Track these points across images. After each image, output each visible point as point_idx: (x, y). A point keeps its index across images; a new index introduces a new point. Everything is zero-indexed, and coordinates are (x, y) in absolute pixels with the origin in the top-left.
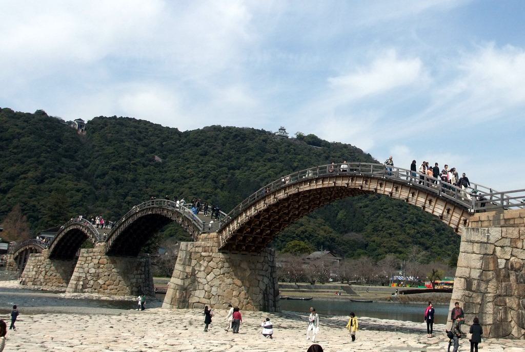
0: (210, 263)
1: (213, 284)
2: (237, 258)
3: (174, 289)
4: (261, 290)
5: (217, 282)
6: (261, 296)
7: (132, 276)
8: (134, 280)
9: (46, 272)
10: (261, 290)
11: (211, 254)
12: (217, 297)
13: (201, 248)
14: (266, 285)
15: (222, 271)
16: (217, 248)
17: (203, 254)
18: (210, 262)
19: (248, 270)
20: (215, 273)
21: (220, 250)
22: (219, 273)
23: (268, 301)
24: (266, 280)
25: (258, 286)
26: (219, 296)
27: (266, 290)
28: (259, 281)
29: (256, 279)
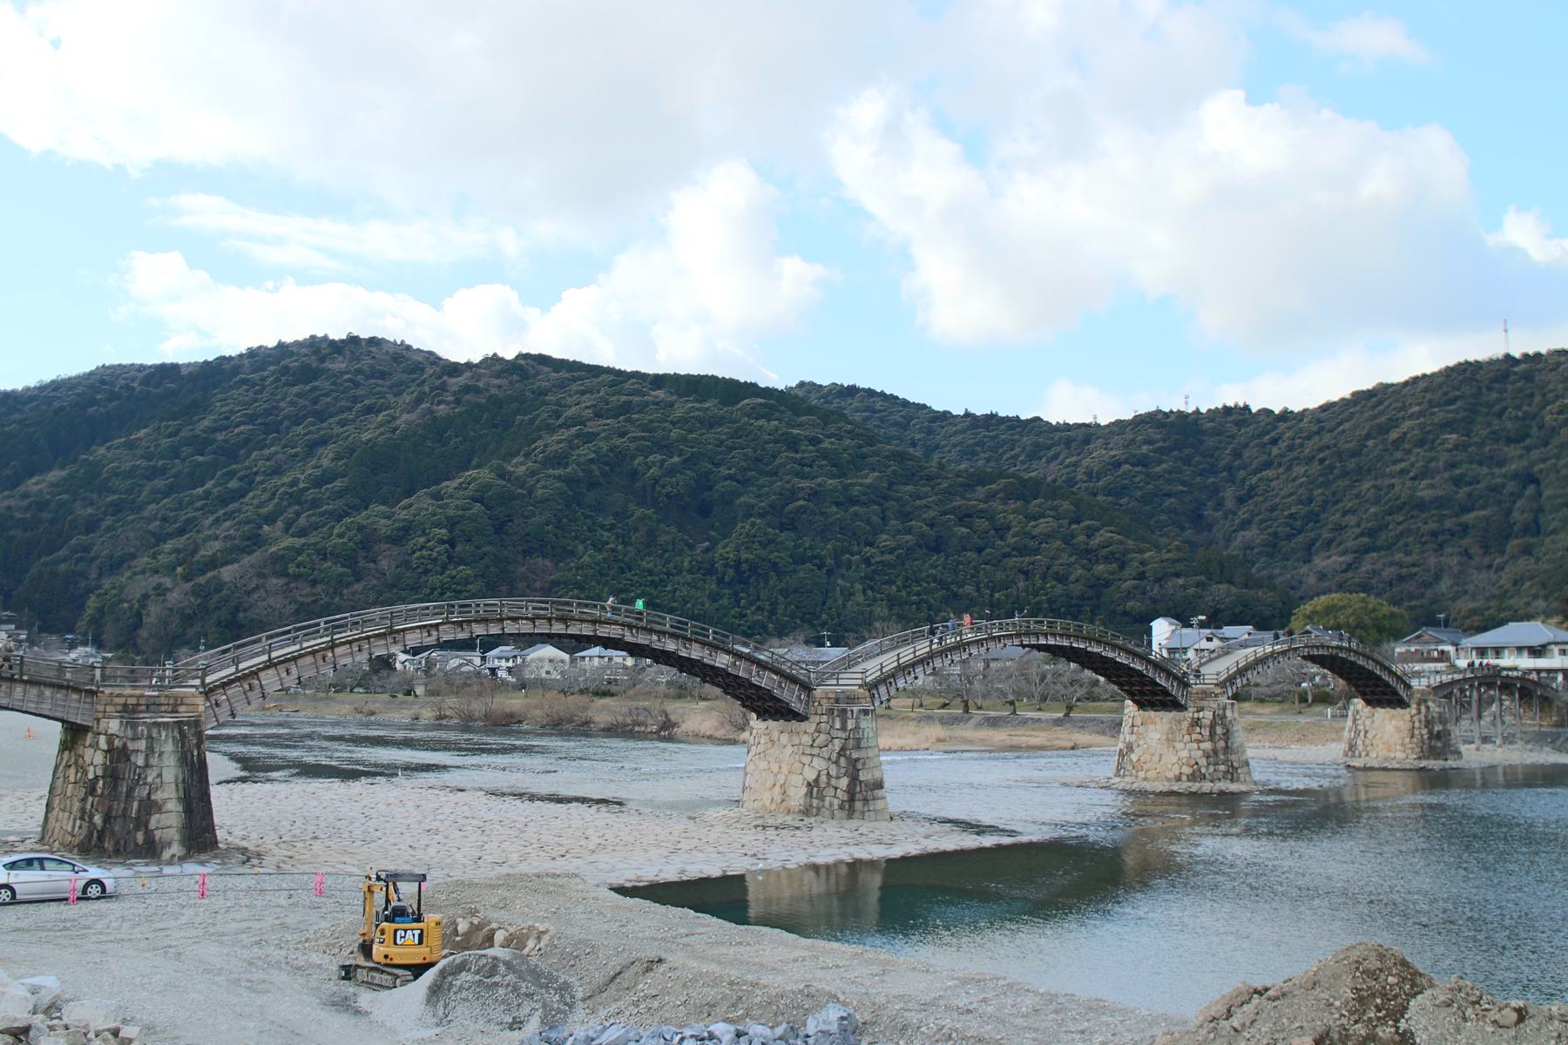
4: (805, 779)
6: (804, 790)
7: (1179, 746)
8: (1185, 754)
9: (1366, 732)
10: (805, 779)
14: (820, 771)
27: (817, 780)
29: (800, 762)
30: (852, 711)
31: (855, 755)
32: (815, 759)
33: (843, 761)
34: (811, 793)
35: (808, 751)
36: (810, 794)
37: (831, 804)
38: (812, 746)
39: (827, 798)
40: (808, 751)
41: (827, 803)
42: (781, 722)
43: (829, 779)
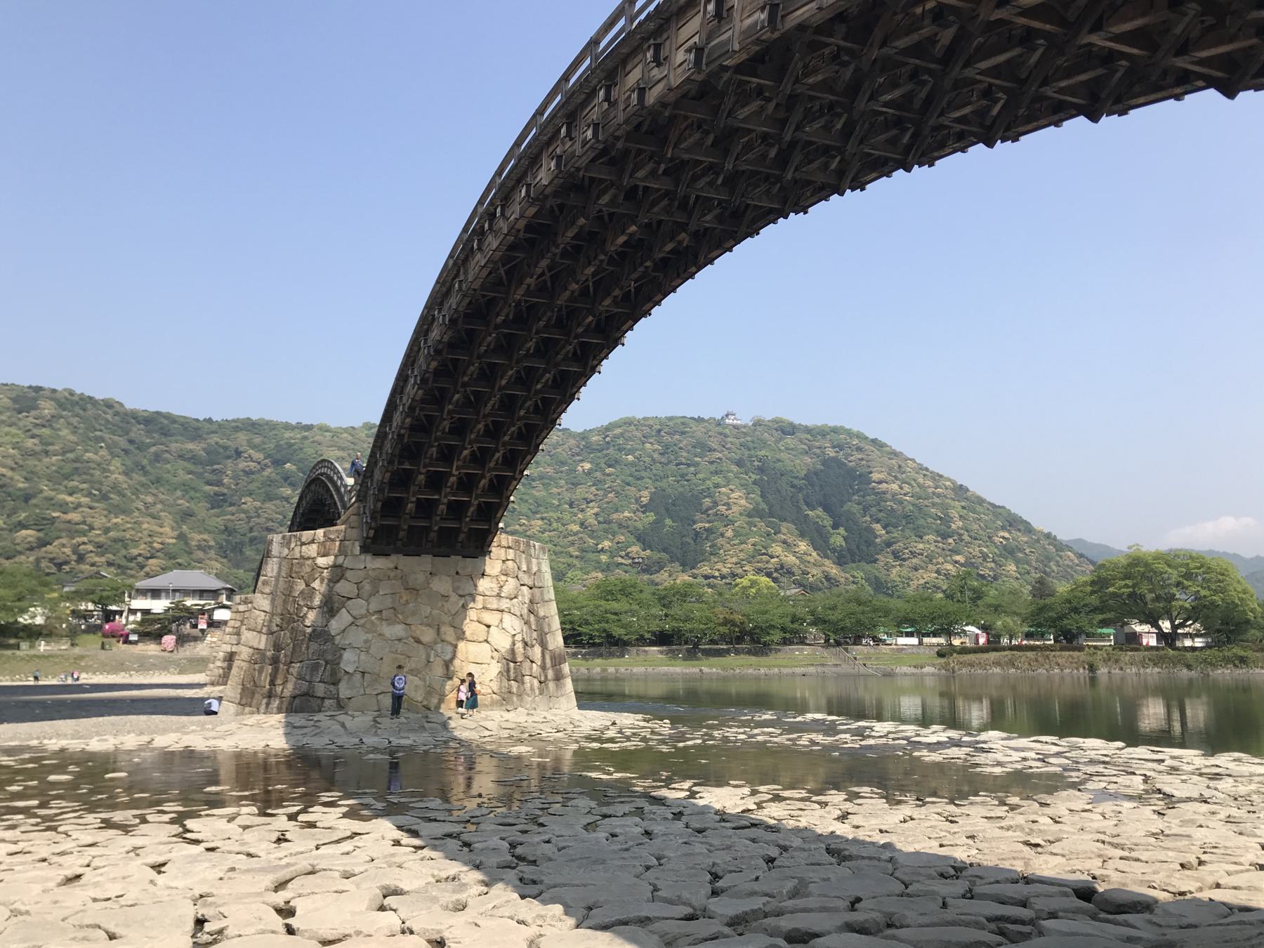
0: (339, 585)
1: (347, 642)
2: (418, 566)
3: (250, 662)
5: (358, 637)
6: (495, 668)
11: (341, 560)
12: (358, 676)
13: (314, 546)
15: (373, 607)
16: (357, 544)
17: (322, 561)
18: (338, 581)
19: (454, 598)
20: (354, 613)
21: (365, 549)
22: (363, 611)
23: (519, 679)
24: (512, 624)
25: (486, 641)
26: (363, 673)
27: (513, 651)
28: (489, 626)
30: (534, 546)
31: (542, 614)
32: (506, 616)
33: (532, 618)
34: (508, 671)
35: (494, 603)
36: (505, 674)
37: (532, 689)
38: (498, 595)
39: (527, 679)
40: (494, 603)
41: (528, 686)
42: (427, 560)
43: (525, 649)
